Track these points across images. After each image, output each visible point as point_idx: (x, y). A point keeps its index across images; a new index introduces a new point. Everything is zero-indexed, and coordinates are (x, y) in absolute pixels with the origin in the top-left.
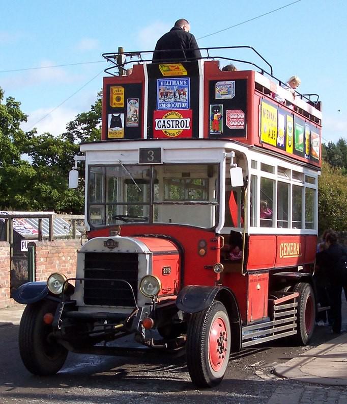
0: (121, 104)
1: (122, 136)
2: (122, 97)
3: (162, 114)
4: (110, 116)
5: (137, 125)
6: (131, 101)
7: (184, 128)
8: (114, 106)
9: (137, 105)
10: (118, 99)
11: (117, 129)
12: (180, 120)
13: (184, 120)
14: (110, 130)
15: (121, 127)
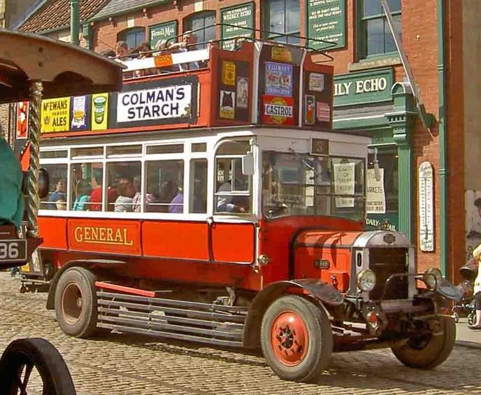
0: (233, 82)
1: (232, 116)
2: (234, 73)
3: (271, 98)
4: (222, 92)
5: (245, 106)
6: (242, 80)
7: (288, 116)
8: (226, 83)
9: (246, 85)
10: (230, 76)
11: (228, 108)
12: (285, 107)
13: (288, 107)
14: (222, 109)
15: (232, 107)
